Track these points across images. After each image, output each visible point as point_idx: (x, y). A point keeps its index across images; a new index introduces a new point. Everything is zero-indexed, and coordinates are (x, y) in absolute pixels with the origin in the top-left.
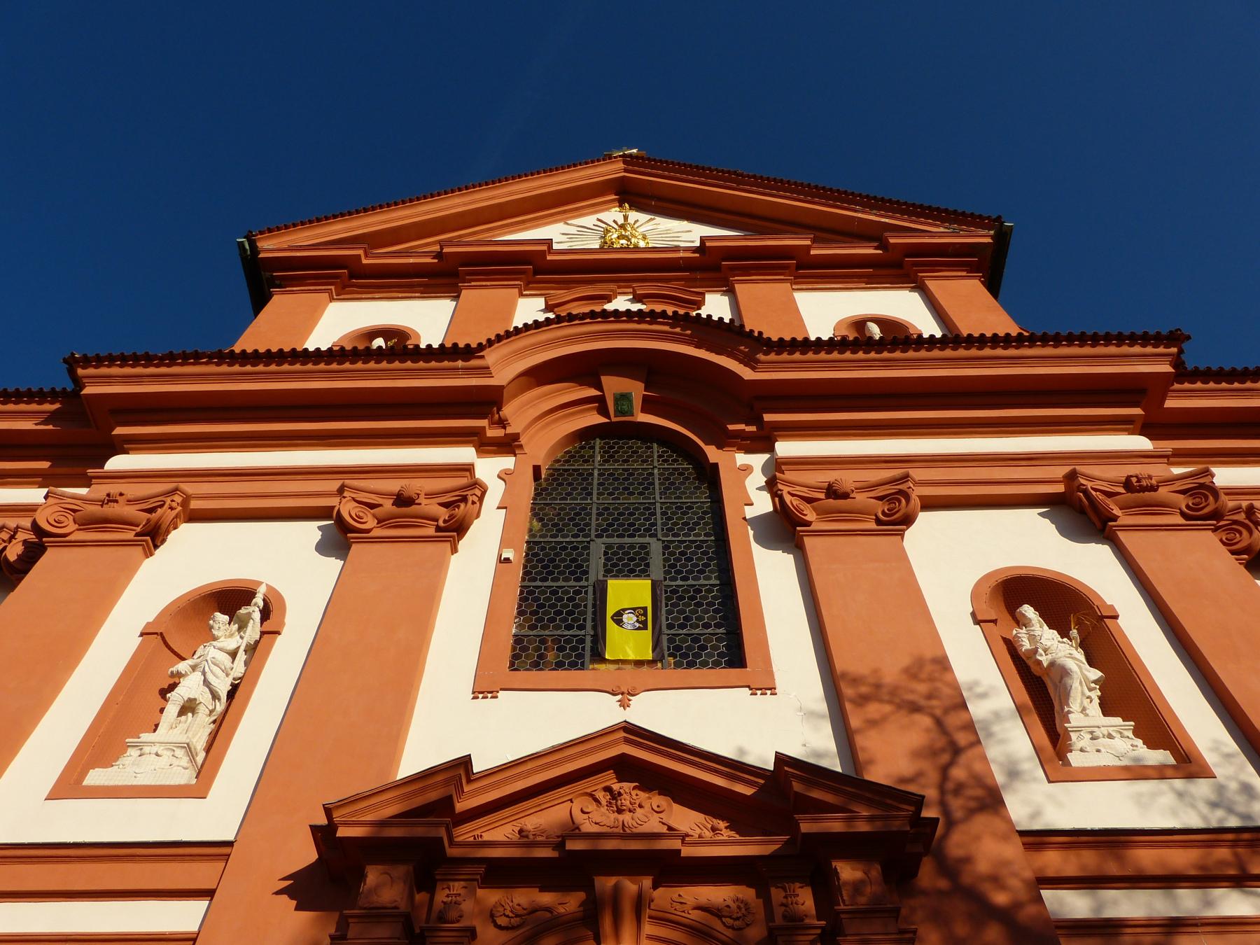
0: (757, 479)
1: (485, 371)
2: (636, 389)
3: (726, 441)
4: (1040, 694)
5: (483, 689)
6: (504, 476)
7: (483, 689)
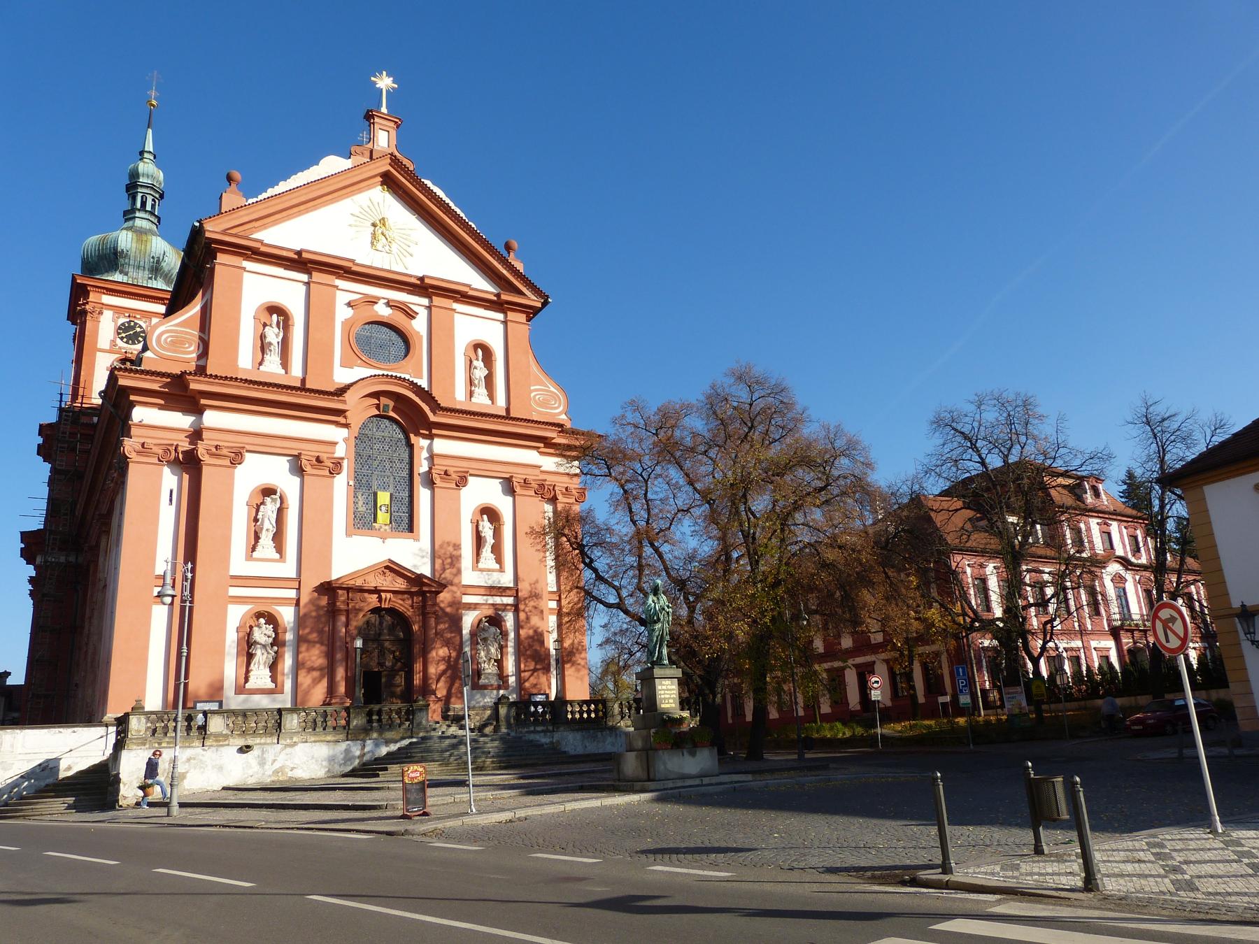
0: (425, 454)
1: (344, 402)
2: (391, 404)
3: (417, 434)
4: (479, 541)
5: (348, 534)
6: (345, 440)
7: (348, 534)
